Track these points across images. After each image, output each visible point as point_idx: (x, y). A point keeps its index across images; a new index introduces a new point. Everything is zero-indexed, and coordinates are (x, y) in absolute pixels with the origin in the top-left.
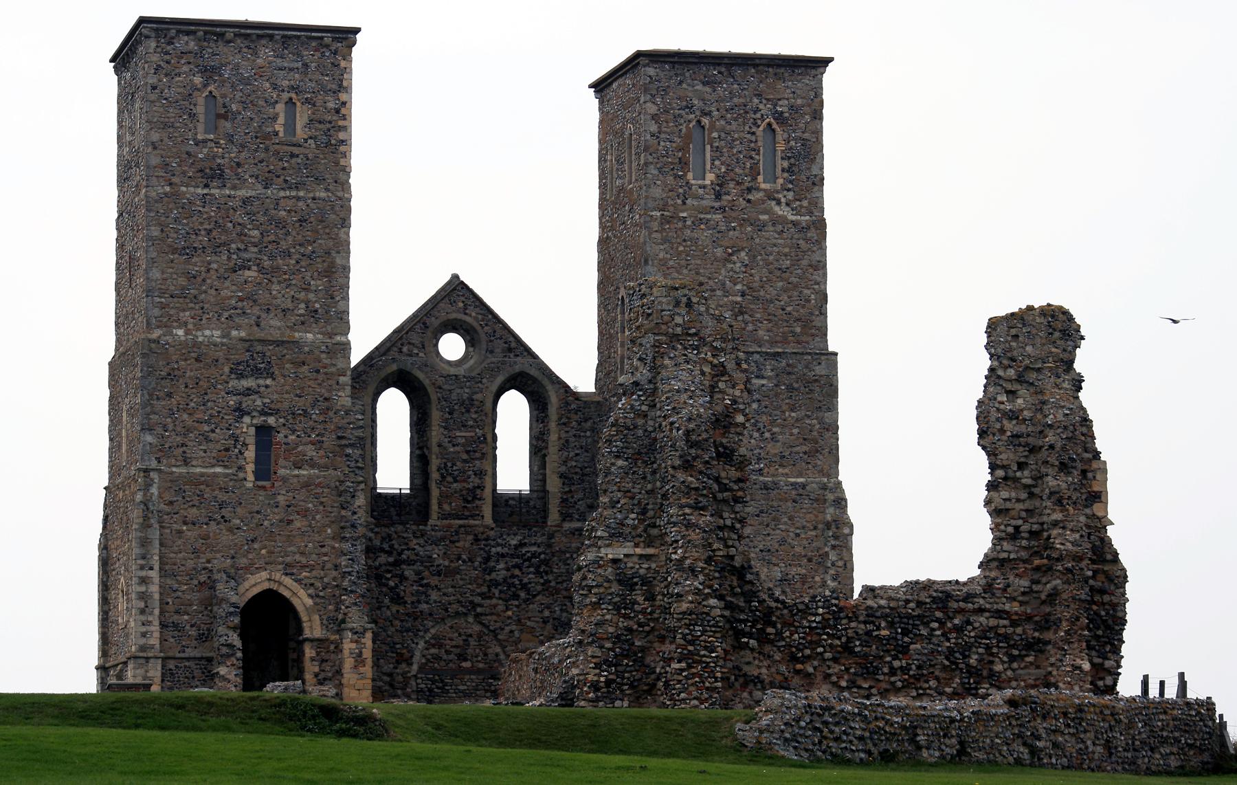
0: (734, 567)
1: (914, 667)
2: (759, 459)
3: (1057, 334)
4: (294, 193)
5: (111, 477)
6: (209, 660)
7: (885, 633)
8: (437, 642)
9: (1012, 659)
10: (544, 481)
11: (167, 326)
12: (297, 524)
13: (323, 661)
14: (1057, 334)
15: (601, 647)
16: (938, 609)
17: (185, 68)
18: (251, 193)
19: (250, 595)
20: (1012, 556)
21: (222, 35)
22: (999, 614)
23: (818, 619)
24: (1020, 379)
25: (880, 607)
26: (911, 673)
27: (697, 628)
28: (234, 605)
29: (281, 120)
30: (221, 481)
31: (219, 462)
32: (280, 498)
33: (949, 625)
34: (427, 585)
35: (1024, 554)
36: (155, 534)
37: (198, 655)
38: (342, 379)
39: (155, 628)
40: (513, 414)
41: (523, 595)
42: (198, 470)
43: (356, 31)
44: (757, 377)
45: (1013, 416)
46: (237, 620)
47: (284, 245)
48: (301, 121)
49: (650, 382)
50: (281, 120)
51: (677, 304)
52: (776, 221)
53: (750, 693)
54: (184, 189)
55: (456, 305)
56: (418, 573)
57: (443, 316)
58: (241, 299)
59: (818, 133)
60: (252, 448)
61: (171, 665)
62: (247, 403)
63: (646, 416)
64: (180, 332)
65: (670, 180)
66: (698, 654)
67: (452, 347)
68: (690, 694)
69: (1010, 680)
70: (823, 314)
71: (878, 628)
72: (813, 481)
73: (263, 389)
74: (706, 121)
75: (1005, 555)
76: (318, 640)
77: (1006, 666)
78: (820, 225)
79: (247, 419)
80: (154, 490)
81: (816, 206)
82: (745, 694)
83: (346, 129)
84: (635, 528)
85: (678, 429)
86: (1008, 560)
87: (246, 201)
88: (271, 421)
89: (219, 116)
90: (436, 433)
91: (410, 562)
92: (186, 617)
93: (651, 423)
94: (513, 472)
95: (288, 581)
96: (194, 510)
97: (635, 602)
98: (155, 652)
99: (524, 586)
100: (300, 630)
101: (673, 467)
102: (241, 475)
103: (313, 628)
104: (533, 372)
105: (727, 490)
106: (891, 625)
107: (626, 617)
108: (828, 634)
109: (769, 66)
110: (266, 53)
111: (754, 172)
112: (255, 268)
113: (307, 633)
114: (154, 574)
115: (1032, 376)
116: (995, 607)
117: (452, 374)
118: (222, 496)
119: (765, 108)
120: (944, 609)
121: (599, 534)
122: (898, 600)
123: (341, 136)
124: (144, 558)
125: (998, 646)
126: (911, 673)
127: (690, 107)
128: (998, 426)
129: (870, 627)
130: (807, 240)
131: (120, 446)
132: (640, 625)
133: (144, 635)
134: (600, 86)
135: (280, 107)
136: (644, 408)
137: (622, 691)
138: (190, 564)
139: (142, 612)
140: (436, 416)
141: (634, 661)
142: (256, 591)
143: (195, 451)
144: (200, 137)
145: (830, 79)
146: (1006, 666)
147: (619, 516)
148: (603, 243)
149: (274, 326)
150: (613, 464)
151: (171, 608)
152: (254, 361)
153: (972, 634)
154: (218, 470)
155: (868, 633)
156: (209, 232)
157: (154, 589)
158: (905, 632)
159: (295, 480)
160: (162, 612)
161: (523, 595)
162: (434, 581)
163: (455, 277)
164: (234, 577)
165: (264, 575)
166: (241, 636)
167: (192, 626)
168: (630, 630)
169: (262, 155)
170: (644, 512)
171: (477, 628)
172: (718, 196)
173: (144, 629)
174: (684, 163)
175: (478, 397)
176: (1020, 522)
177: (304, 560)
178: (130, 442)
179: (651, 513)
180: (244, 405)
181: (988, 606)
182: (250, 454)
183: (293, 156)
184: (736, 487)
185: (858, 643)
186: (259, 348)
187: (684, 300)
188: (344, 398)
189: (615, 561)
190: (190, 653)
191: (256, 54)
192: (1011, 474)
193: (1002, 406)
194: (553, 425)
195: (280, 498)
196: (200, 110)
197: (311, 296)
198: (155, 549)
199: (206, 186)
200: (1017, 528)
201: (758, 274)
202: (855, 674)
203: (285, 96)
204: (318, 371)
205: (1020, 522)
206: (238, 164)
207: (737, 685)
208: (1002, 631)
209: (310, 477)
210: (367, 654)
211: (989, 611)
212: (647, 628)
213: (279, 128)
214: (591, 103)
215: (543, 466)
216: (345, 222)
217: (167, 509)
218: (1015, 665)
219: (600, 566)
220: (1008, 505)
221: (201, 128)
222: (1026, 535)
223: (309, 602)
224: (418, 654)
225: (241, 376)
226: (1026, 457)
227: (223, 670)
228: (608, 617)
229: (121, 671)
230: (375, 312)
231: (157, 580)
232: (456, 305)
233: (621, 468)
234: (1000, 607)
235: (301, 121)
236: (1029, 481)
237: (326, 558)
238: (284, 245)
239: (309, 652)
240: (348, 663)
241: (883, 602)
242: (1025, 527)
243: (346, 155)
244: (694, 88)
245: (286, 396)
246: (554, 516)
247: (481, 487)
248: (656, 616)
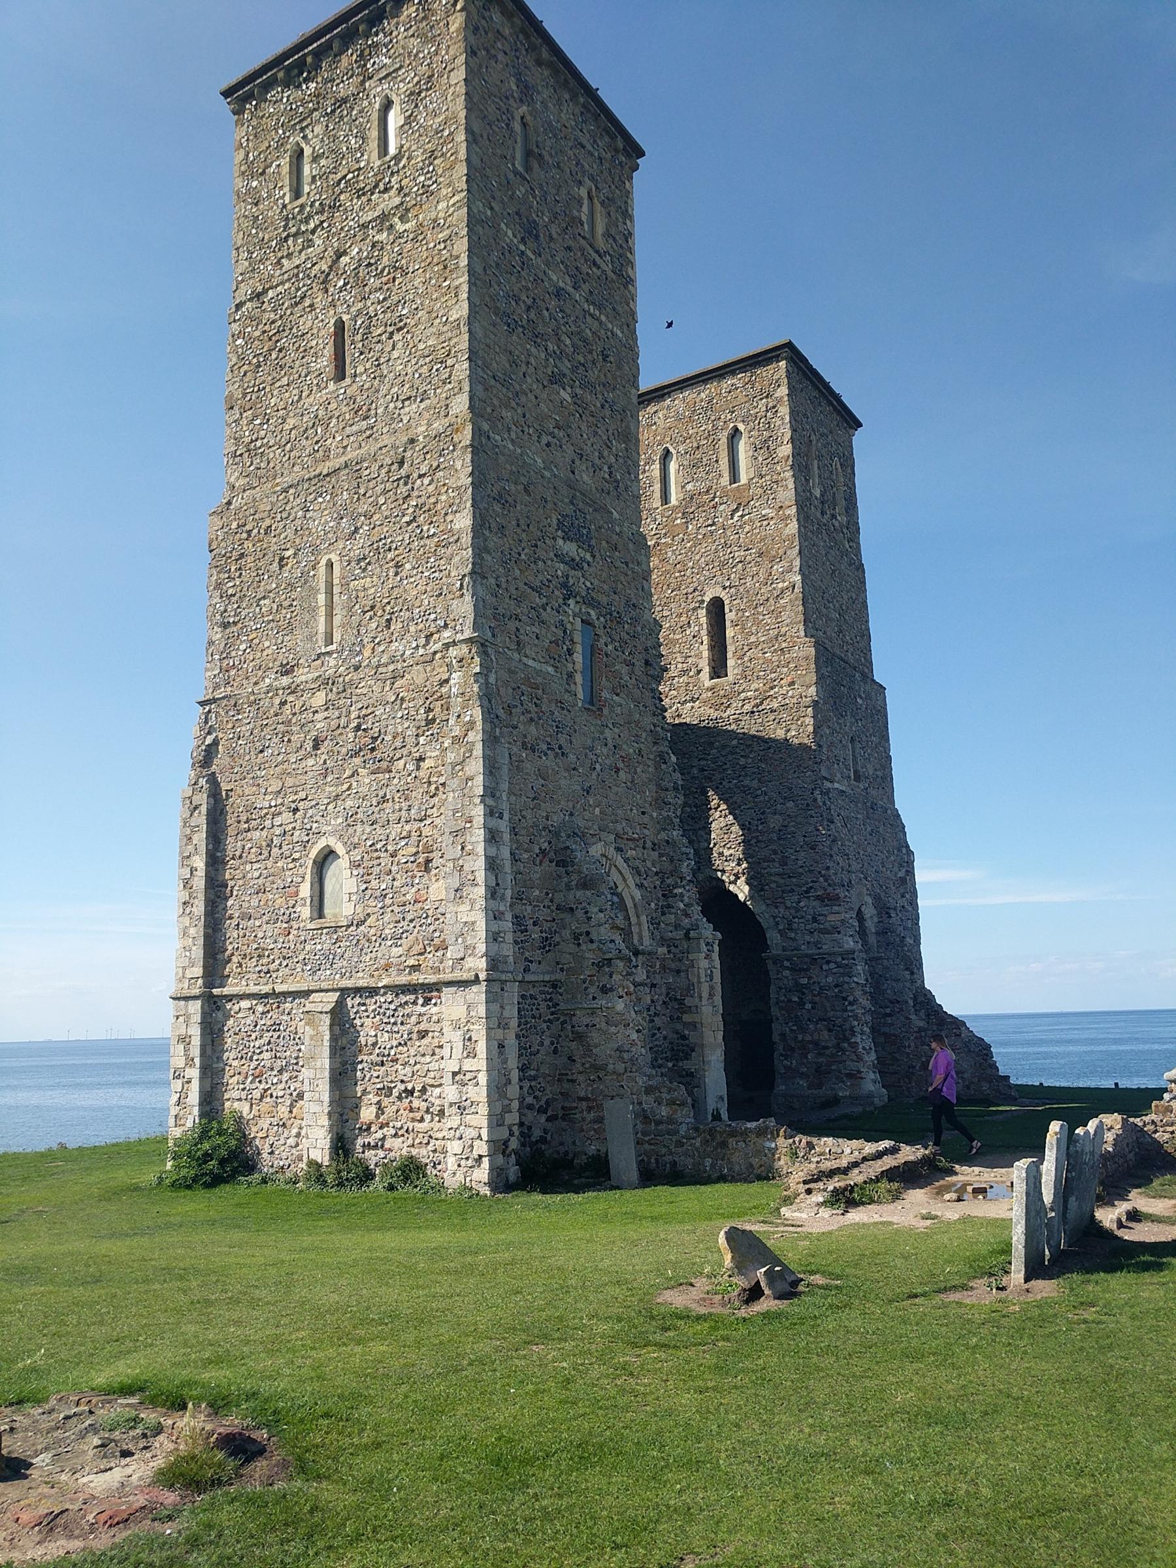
4: (597, 313)
18: (561, 284)
29: (585, 208)
32: (608, 733)
37: (547, 978)
39: (507, 925)
42: (530, 662)
50: (585, 208)
54: (503, 226)
60: (579, 648)
73: (585, 566)
74: (813, 437)
78: (860, 567)
79: (571, 602)
83: (631, 264)
87: (559, 293)
92: (529, 908)
109: (835, 408)
112: (569, 389)
135: (583, 192)
157: (506, 853)
159: (618, 710)
167: (535, 924)
172: (822, 514)
173: (495, 928)
180: (571, 581)
182: (578, 657)
183: (595, 263)
186: (581, 505)
195: (608, 733)
196: (517, 127)
199: (523, 241)
204: (627, 564)
213: (584, 218)
223: (638, 894)
229: (340, 1005)
231: (506, 837)
237: (646, 832)
245: (605, 587)
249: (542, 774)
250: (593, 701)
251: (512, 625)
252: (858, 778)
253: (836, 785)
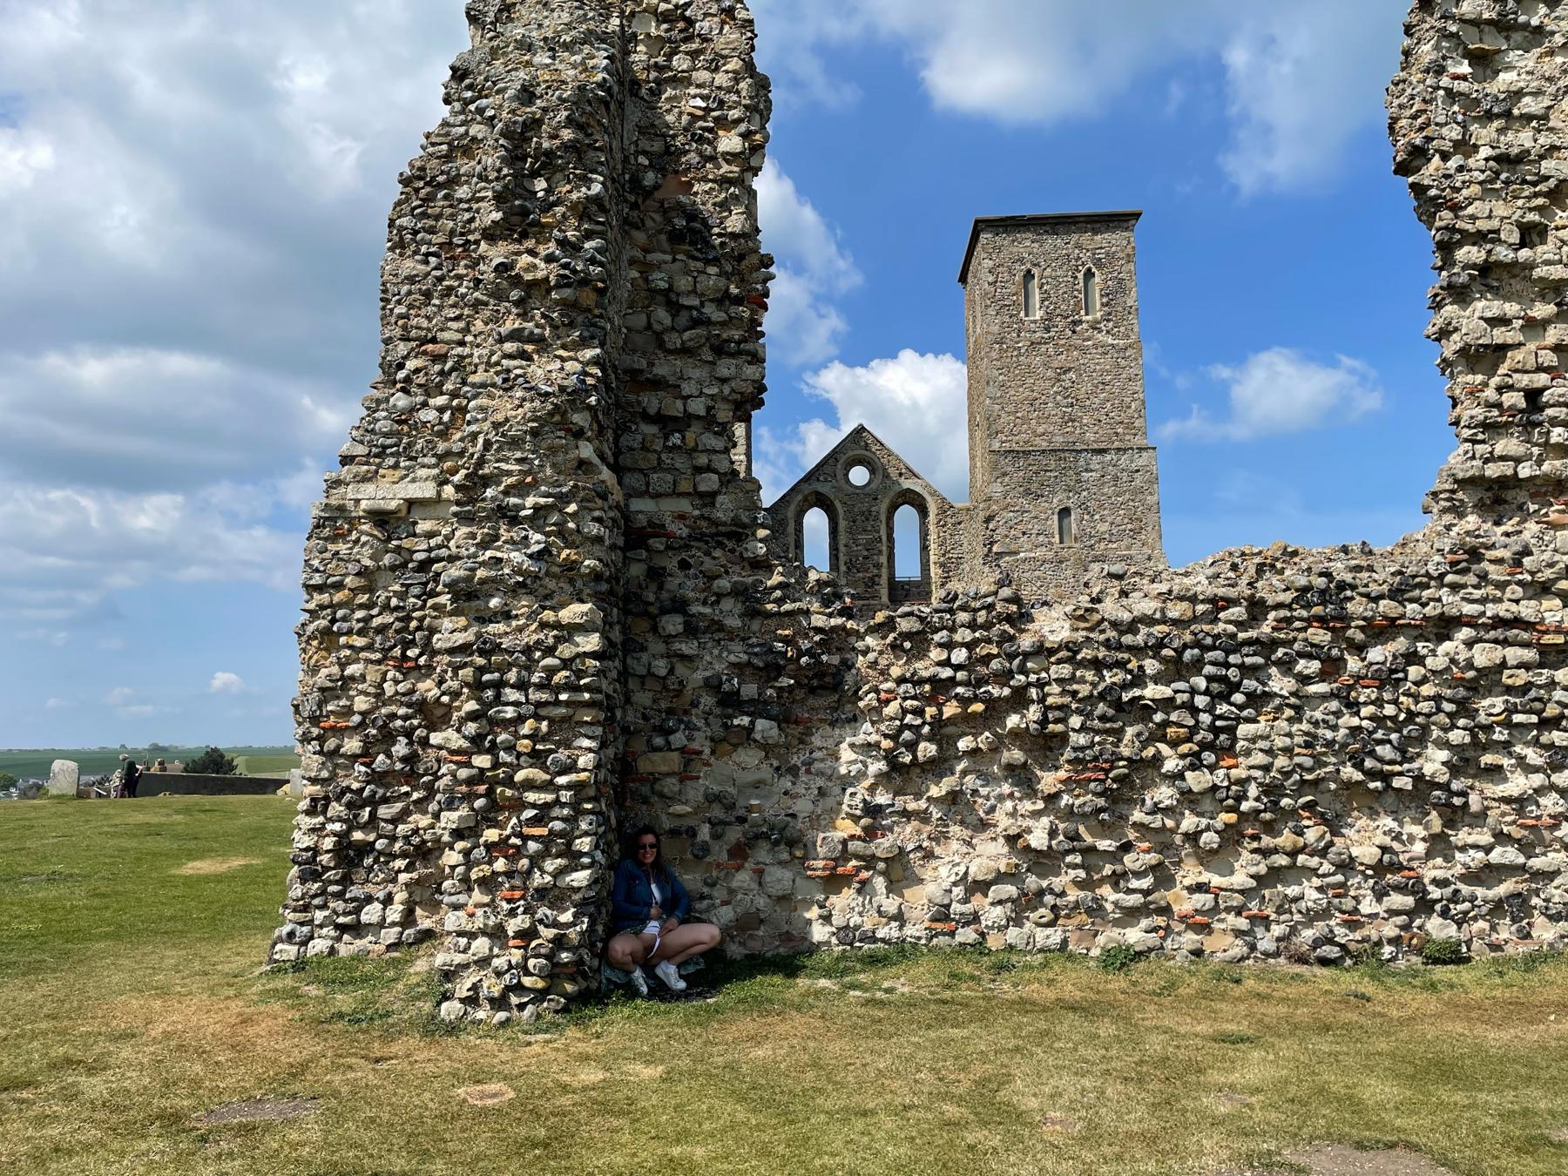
0: (715, 523)
1: (1253, 791)
16: (1322, 621)
20: (1525, 471)
23: (959, 656)
26: (1245, 806)
33: (1353, 664)
44: (1087, 470)
53: (759, 873)
57: (851, 453)
65: (1007, 319)
66: (509, 782)
67: (859, 475)
71: (1139, 679)
74: (1035, 271)
75: (1506, 469)
77: (1538, 780)
82: (743, 878)
104: (918, 489)
105: (696, 323)
108: (990, 702)
116: (1491, 609)
120: (1337, 622)
122: (1193, 600)
125: (1508, 724)
126: (1245, 806)
128: (1454, 133)
129: (1111, 677)
140: (842, 524)
146: (1538, 780)
147: (401, 401)
153: (1427, 690)
158: (1224, 689)
176: (1542, 379)
181: (1468, 609)
184: (717, 315)
185: (1075, 721)
189: (381, 518)
192: (1503, 253)
193: (1462, 86)
200: (1533, 395)
205: (1542, 379)
207: (720, 854)
211: (1471, 622)
220: (1500, 335)
226: (1539, 209)
234: (1503, 610)
244: (1025, 245)
247: (879, 576)
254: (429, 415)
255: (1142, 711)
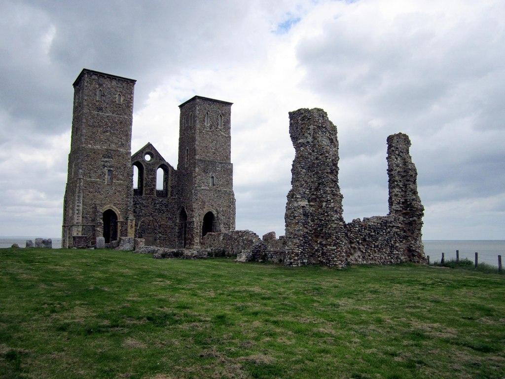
2: (218, 185)
3: (406, 142)
5: (68, 181)
6: (94, 226)
7: (373, 234)
8: (143, 222)
9: (401, 242)
10: (167, 187)
11: (87, 144)
12: (117, 194)
13: (122, 227)
14: (406, 142)
15: (299, 240)
17: (94, 83)
19: (105, 210)
21: (104, 76)
22: (398, 228)
24: (398, 155)
25: (372, 225)
27: (339, 233)
28: (101, 213)
30: (99, 183)
31: (98, 177)
34: (142, 209)
35: (401, 209)
36: (82, 195)
38: (129, 160)
39: (81, 218)
40: (160, 172)
41: (162, 212)
43: (136, 81)
45: (397, 166)
46: (102, 217)
47: (116, 128)
48: (122, 99)
49: (312, 142)
51: (320, 116)
52: (222, 135)
55: (149, 149)
56: (140, 206)
57: (147, 151)
58: (105, 139)
59: (230, 118)
61: (84, 227)
62: (106, 164)
63: (311, 154)
64: (90, 146)
67: (148, 158)
68: (338, 258)
69: (400, 248)
70: (230, 155)
72: (228, 190)
74: (208, 112)
75: (397, 209)
76: (122, 222)
78: (230, 137)
80: (82, 184)
81: (229, 133)
84: (308, 195)
85: (329, 159)
86: (398, 210)
88: (112, 169)
89: (102, 95)
90: (145, 176)
91: (138, 204)
93: (313, 157)
94: (160, 185)
95: (114, 207)
96: (92, 189)
97: (309, 223)
98: (81, 224)
99: (162, 210)
100: (117, 219)
101: (327, 173)
102: (104, 181)
103: (120, 219)
104: (166, 164)
106: (375, 231)
107: (306, 228)
110: (114, 83)
111: (218, 125)
113: (119, 220)
114: (81, 205)
115: (401, 154)
117: (148, 164)
118: (99, 186)
119: (220, 112)
120: (386, 226)
121: (298, 196)
123: (131, 104)
124: (78, 200)
127: (205, 109)
130: (227, 140)
131: (71, 173)
132: (310, 231)
133: (78, 220)
134: (181, 106)
135: (117, 96)
136: (311, 151)
137: (305, 255)
138: (90, 202)
139: (78, 214)
140: (145, 172)
141: (308, 244)
142: (106, 209)
143: (93, 175)
144: (97, 100)
145: (232, 107)
148: (180, 139)
149: (113, 146)
150: (301, 171)
151: (85, 213)
152: (108, 154)
154: (98, 180)
155: (369, 234)
156: (98, 122)
157: (81, 208)
160: (83, 214)
161: (162, 212)
162: (143, 208)
163: (149, 143)
164: (102, 205)
165: (109, 206)
166: (103, 220)
168: (307, 233)
169: (112, 106)
170: (311, 189)
171: (152, 219)
172: (210, 129)
174: (204, 121)
175: (154, 169)
177: (118, 203)
178: (74, 172)
179: (313, 190)
187: (322, 115)
188: (129, 165)
189: (303, 207)
190: (89, 224)
191: (112, 82)
194: (170, 176)
197: (122, 140)
198: (81, 199)
201: (218, 146)
202: (366, 248)
203: (118, 93)
205: (399, 199)
206: (106, 108)
208: (398, 233)
209: (121, 183)
210: (134, 225)
212: (312, 232)
214: (178, 111)
215: (167, 184)
216: (131, 124)
217: (85, 188)
218: (401, 244)
219: (299, 209)
221: (97, 98)
222: (401, 203)
224: (139, 224)
225: (105, 158)
227: (98, 229)
228: (301, 228)
230: (136, 146)
232: (149, 149)
233: (304, 172)
235: (122, 99)
236: (401, 186)
238: (116, 128)
239: (119, 224)
240: (129, 227)
241: (372, 223)
242: (401, 201)
243: (132, 109)
246: (169, 195)
248: (315, 228)
249: (95, 196)
250: (111, 184)
251: (89, 174)
252: (214, 185)
253: (202, 188)
254: (306, 192)
255: (372, 236)
